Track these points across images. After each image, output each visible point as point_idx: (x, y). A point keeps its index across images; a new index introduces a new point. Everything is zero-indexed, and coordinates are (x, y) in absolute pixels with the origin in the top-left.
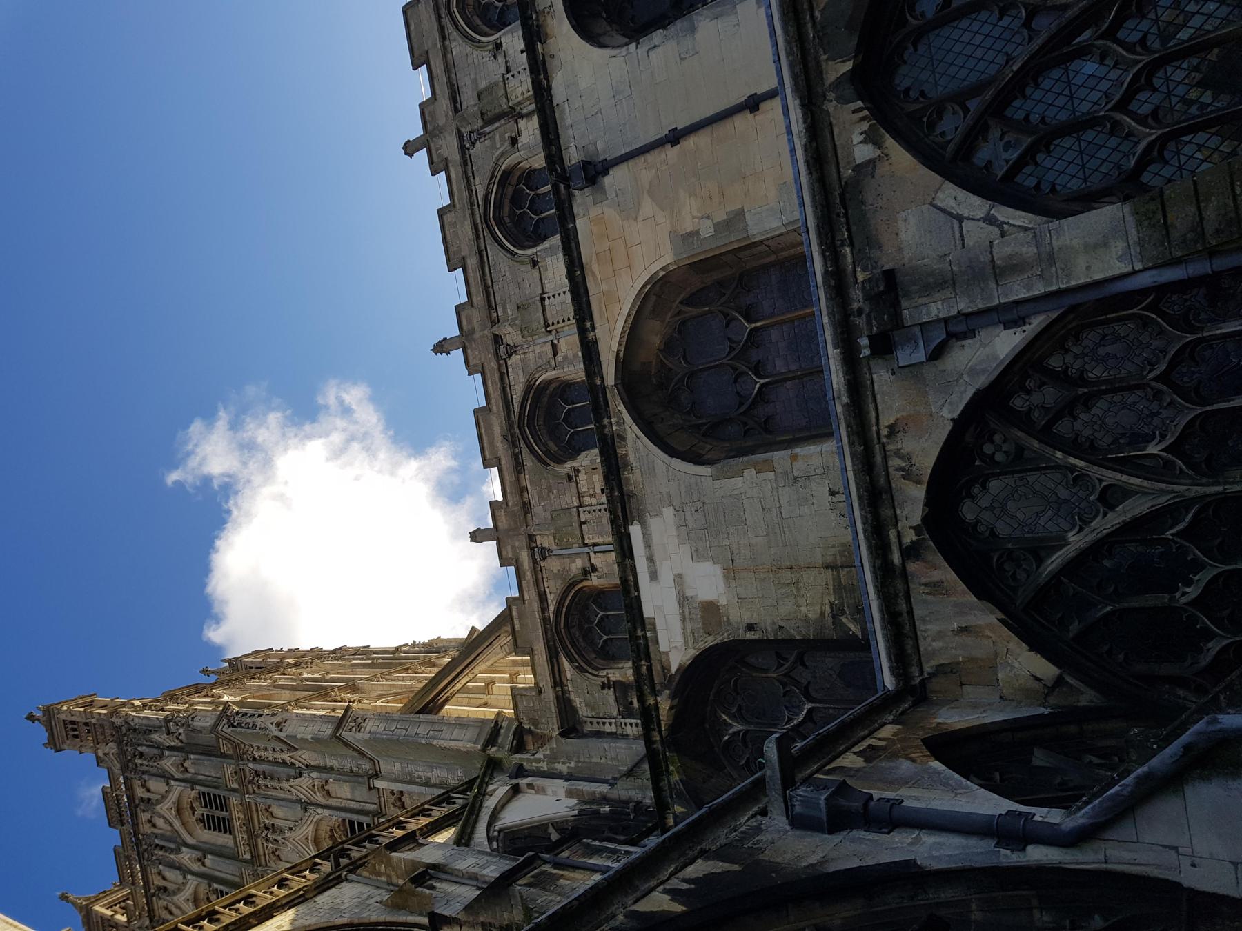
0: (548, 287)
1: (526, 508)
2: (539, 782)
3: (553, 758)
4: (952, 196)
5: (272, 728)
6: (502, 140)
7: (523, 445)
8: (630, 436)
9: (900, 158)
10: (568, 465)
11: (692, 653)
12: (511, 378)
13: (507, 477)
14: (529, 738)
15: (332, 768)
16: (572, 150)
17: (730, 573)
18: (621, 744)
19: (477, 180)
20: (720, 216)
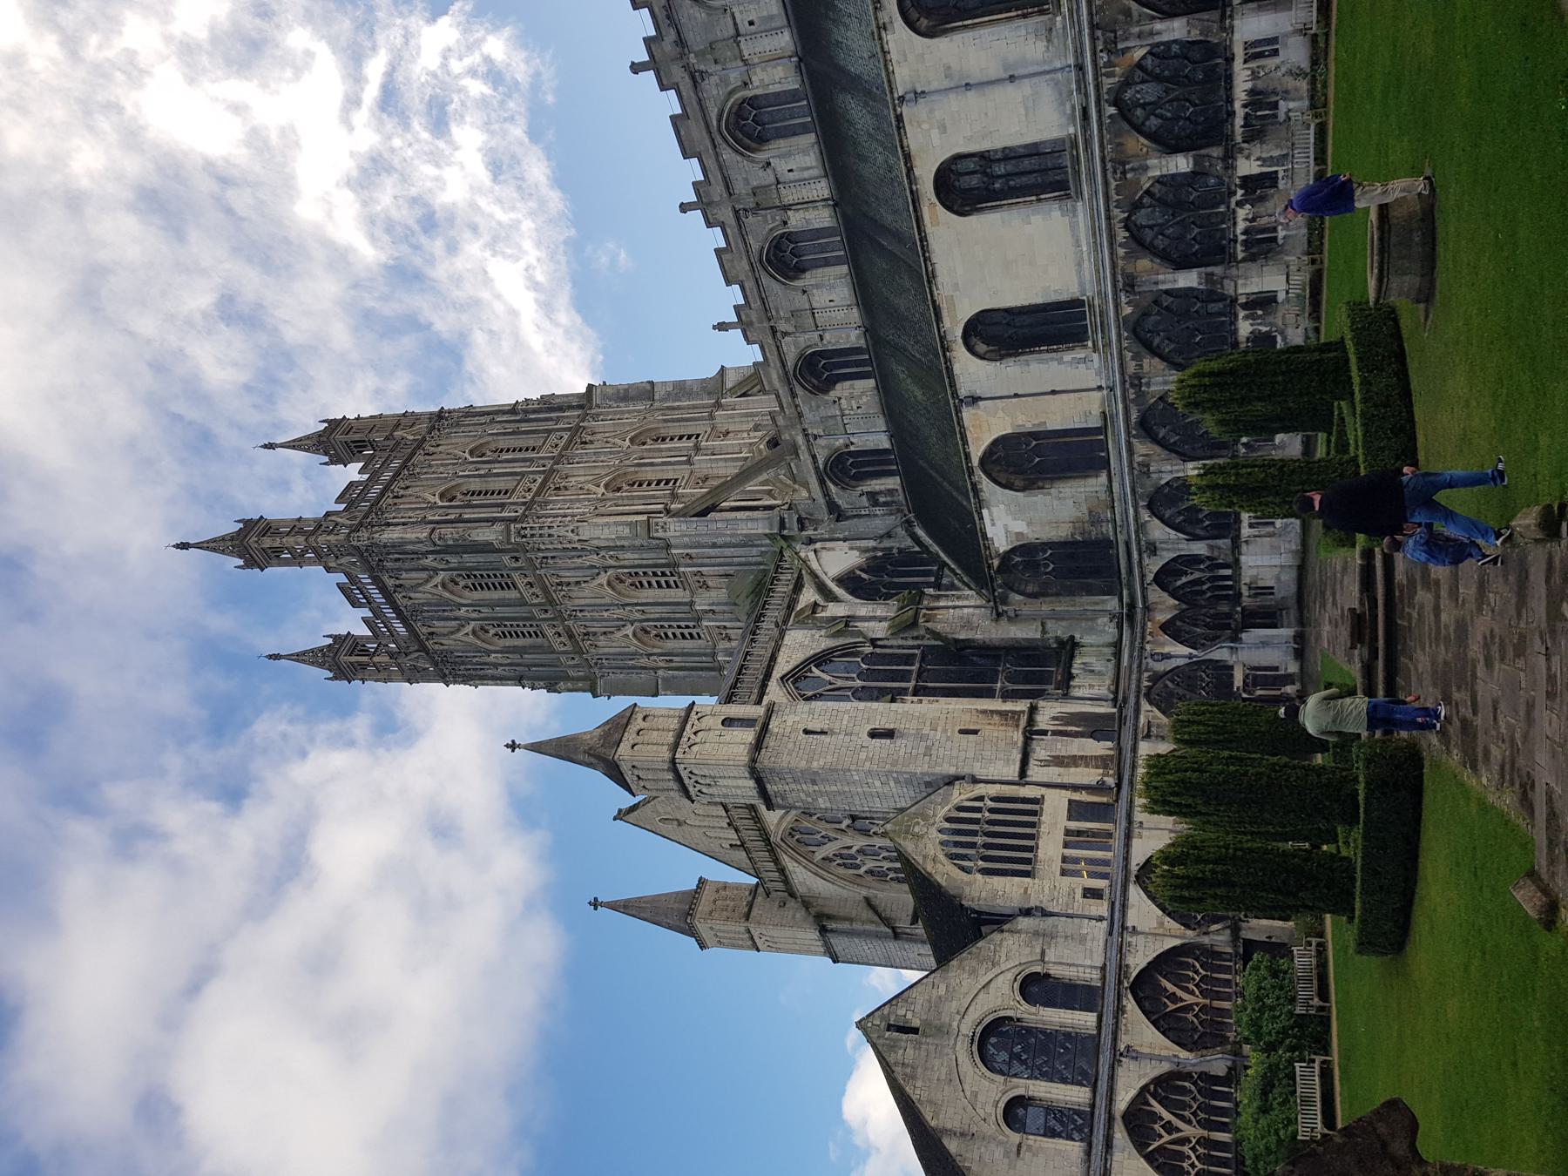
0: (814, 305)
1: (800, 415)
2: (828, 544)
3: (832, 531)
4: (1167, 529)
5: (570, 534)
6: (774, 220)
7: (795, 382)
8: (984, 483)
9: (1156, 521)
10: (832, 393)
11: (1010, 547)
12: (785, 349)
13: (784, 400)
14: (807, 523)
15: (623, 546)
16: (963, 391)
17: (1029, 524)
18: (878, 521)
19: (750, 237)
20: (1036, 422)
